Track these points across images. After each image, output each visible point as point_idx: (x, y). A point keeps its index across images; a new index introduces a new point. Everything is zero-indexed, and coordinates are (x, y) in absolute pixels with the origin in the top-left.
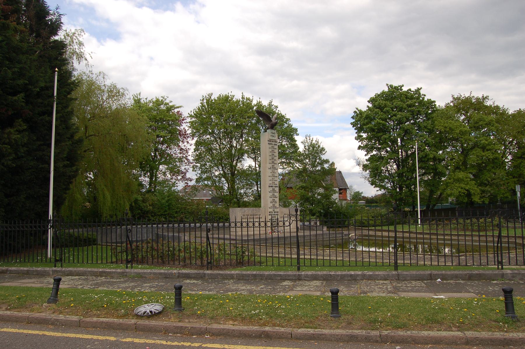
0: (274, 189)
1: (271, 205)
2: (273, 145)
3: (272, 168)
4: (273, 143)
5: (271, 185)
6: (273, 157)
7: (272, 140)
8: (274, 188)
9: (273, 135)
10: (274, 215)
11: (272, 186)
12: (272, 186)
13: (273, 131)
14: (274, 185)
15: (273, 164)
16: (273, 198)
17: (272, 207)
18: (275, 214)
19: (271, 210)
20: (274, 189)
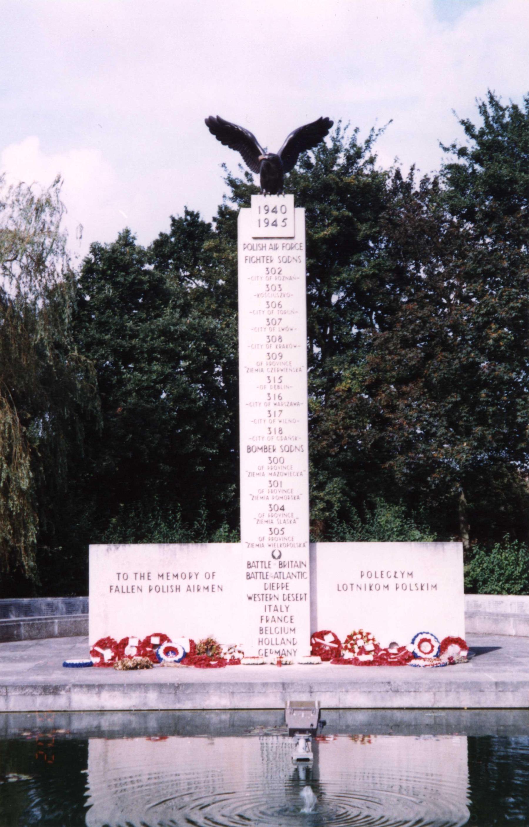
0: (282, 460)
1: (264, 530)
2: (276, 264)
3: (264, 367)
4: (274, 254)
5: (261, 444)
6: (276, 315)
7: (268, 242)
8: (278, 454)
9: (271, 217)
10: (278, 575)
11: (265, 449)
12: (265, 449)
13: (273, 200)
14: (277, 443)
15: (273, 350)
16: (273, 502)
17: (266, 542)
18: (285, 570)
19: (264, 554)
20: (282, 460)
